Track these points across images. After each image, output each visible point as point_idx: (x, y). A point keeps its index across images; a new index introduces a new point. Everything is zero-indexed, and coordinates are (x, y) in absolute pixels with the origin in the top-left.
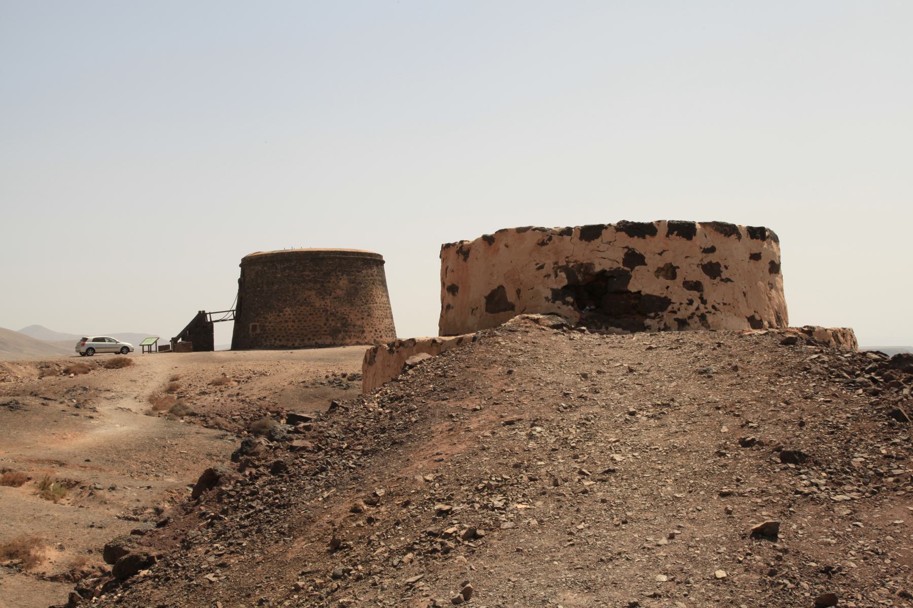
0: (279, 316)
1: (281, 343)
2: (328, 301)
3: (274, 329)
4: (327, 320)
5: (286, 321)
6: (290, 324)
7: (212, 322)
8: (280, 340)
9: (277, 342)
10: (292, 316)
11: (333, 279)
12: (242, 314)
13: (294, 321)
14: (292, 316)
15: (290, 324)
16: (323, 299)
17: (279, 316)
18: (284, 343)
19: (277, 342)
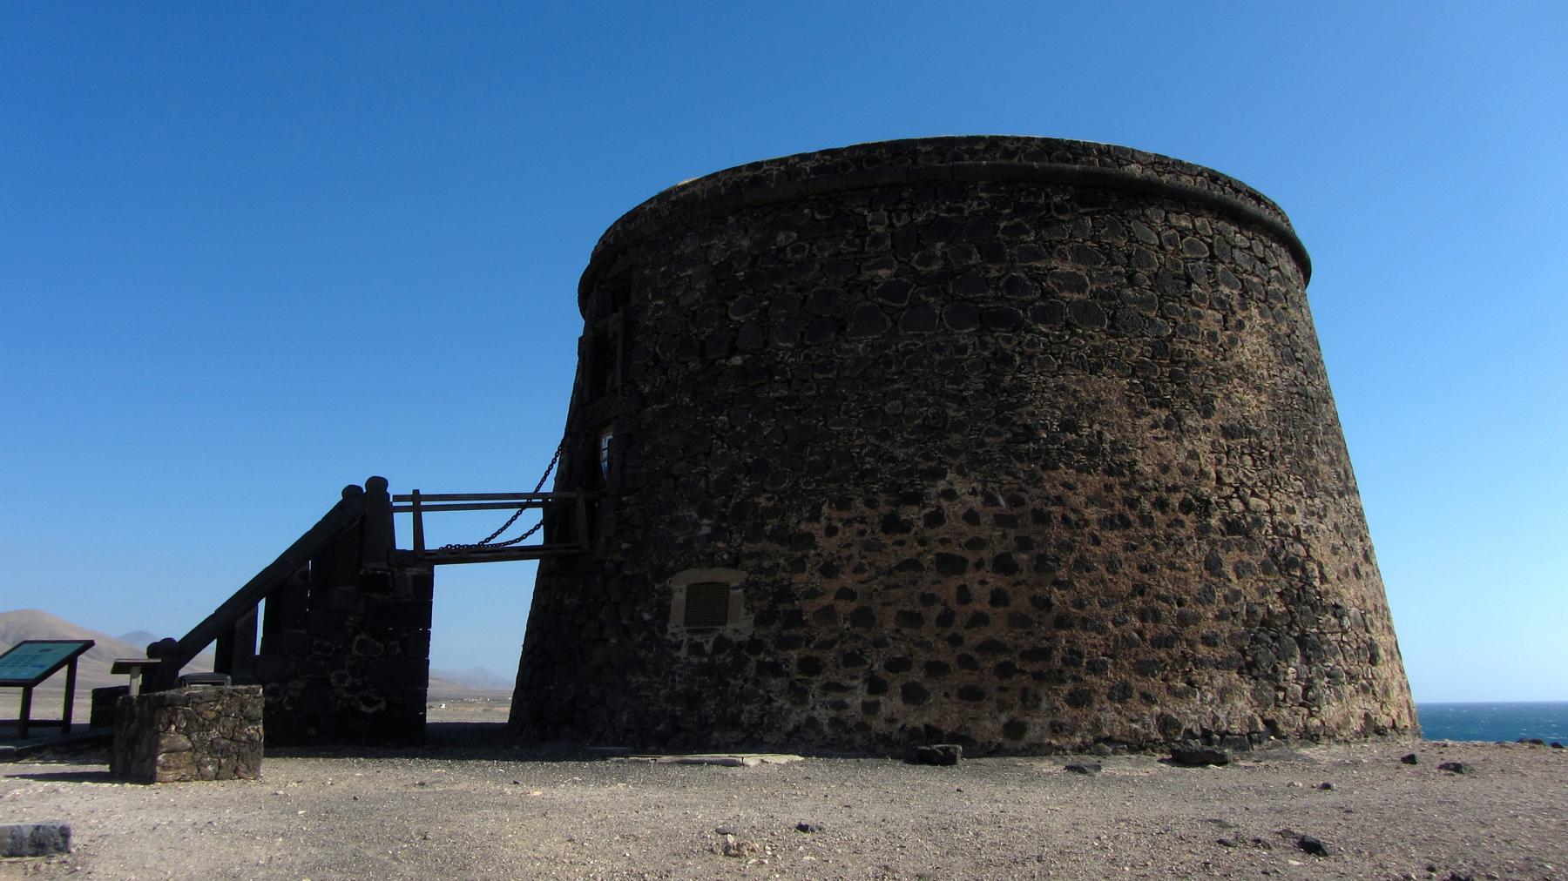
0: (892, 524)
1: (917, 719)
2: (1203, 444)
3: (864, 617)
4: (1213, 565)
5: (950, 565)
6: (981, 582)
7: (425, 561)
8: (913, 695)
9: (891, 704)
10: (986, 530)
11: (1211, 319)
12: (589, 538)
13: (1004, 565)
14: (986, 530)
15: (981, 582)
16: (1174, 423)
17: (892, 524)
18: (943, 712)
19: (891, 704)
